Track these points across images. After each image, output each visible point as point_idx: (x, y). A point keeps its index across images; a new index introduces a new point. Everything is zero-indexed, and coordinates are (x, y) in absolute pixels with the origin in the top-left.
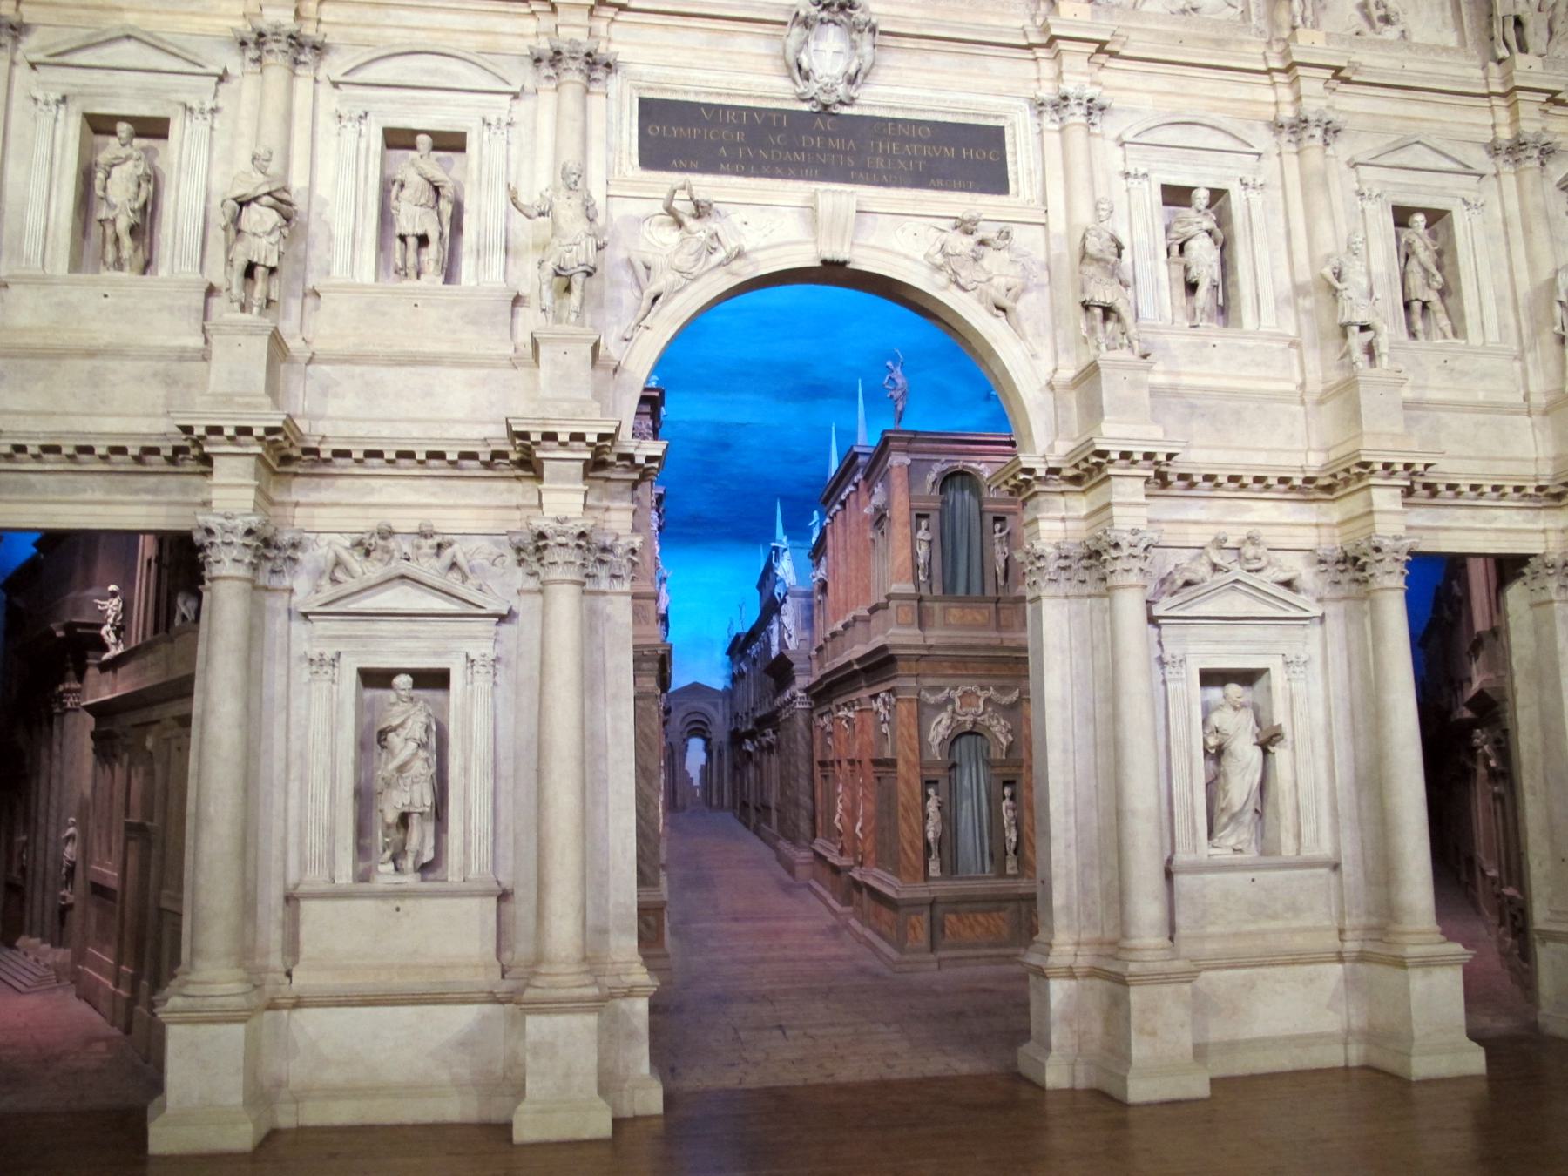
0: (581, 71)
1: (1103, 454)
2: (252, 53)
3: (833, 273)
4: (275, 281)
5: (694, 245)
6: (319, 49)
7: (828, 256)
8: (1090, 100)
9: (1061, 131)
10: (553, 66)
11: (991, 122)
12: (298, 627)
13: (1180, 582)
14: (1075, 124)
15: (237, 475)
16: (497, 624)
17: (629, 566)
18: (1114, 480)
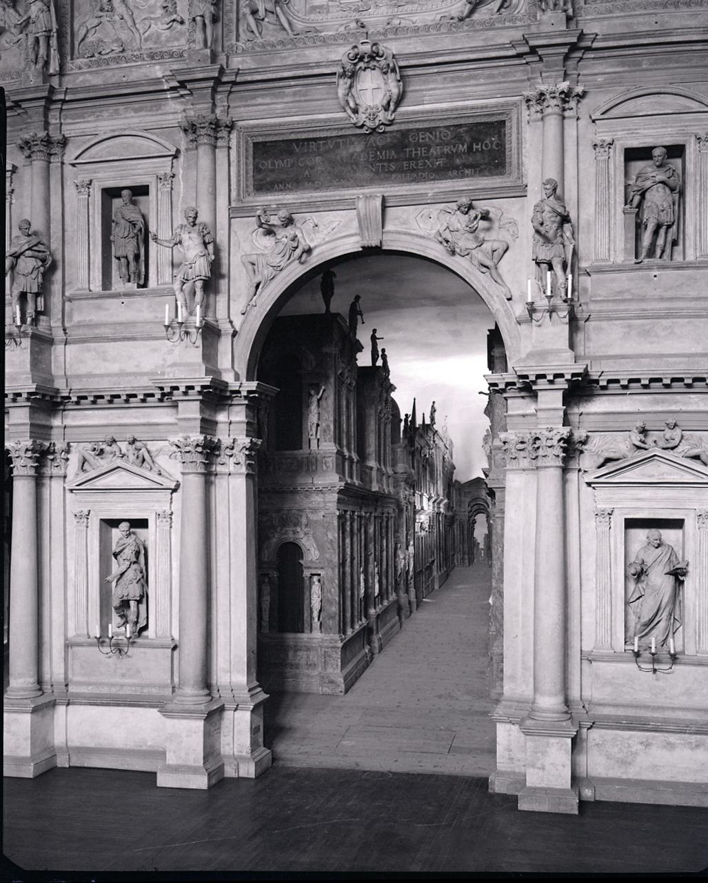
0: (209, 135)
1: (526, 377)
2: (27, 152)
3: (372, 252)
4: (41, 301)
5: (281, 247)
6: (64, 142)
7: (366, 243)
8: (562, 92)
9: (542, 119)
10: (194, 133)
11: (494, 119)
12: (68, 494)
13: (601, 460)
14: (549, 115)
15: (21, 418)
16: (172, 493)
17: (244, 457)
18: (540, 394)
